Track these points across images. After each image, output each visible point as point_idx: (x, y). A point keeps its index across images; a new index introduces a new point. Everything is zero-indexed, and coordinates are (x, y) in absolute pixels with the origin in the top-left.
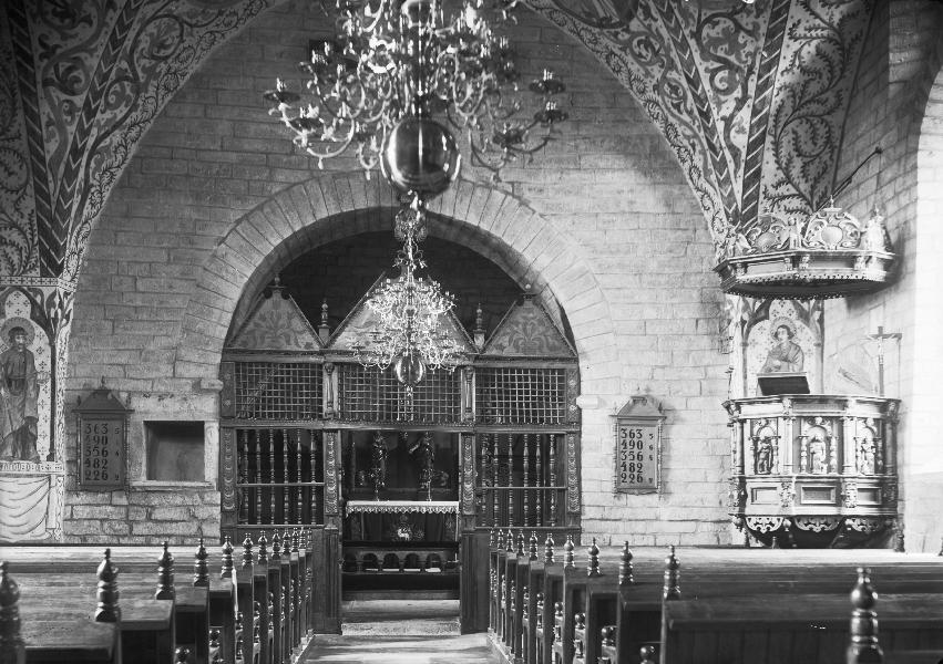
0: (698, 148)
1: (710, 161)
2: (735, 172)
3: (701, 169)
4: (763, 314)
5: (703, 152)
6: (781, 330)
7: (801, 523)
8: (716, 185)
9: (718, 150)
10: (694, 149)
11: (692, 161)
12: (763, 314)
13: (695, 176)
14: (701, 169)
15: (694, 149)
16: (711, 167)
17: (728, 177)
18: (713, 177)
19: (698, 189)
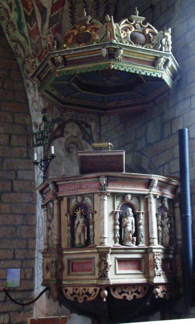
0: (14, 7)
1: (23, 16)
2: (42, 25)
3: (15, 24)
4: (59, 133)
5: (18, 10)
6: (72, 145)
7: (116, 292)
8: (27, 35)
9: (30, 7)
10: (11, 8)
11: (9, 17)
12: (59, 133)
13: (11, 30)
14: (15, 24)
15: (11, 8)
16: (23, 20)
17: (37, 28)
18: (25, 30)
19: (13, 41)
